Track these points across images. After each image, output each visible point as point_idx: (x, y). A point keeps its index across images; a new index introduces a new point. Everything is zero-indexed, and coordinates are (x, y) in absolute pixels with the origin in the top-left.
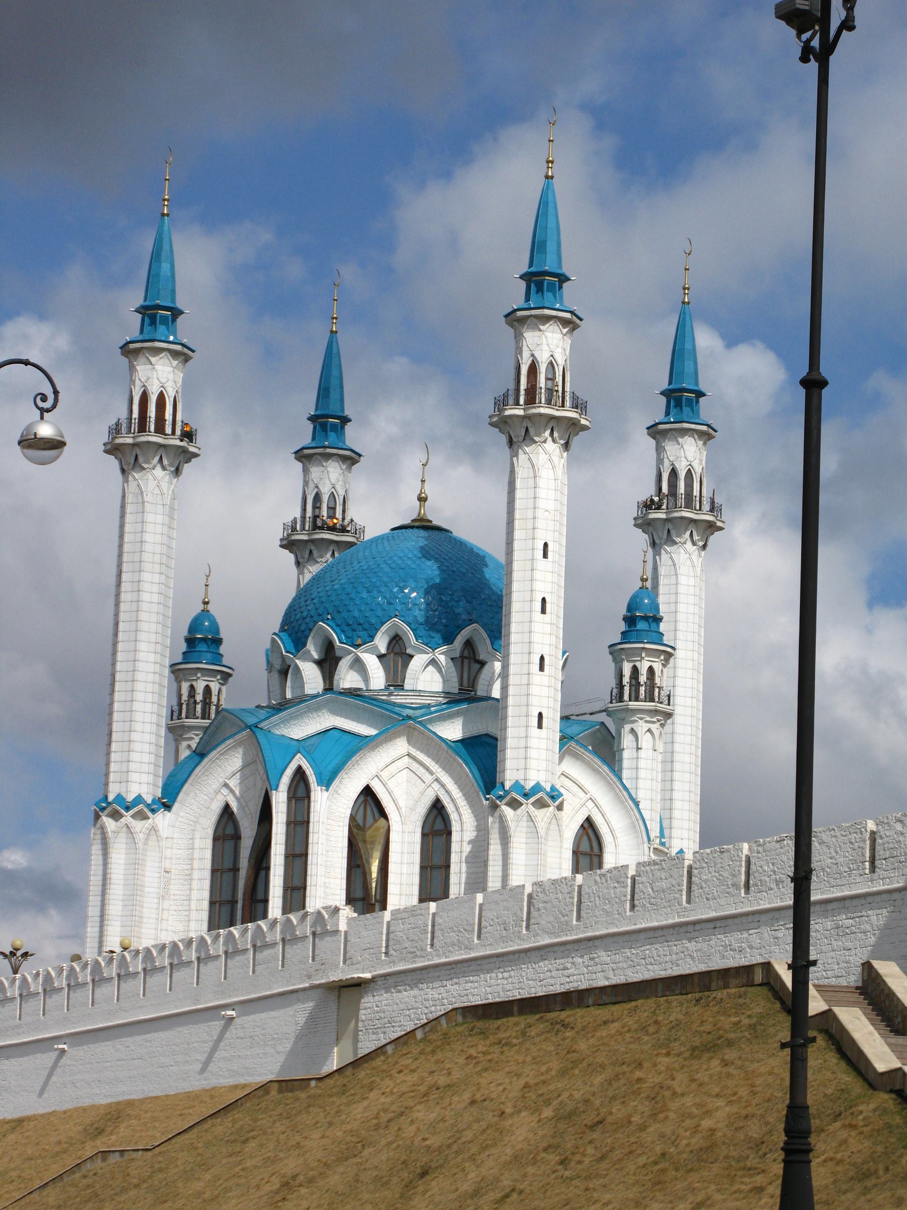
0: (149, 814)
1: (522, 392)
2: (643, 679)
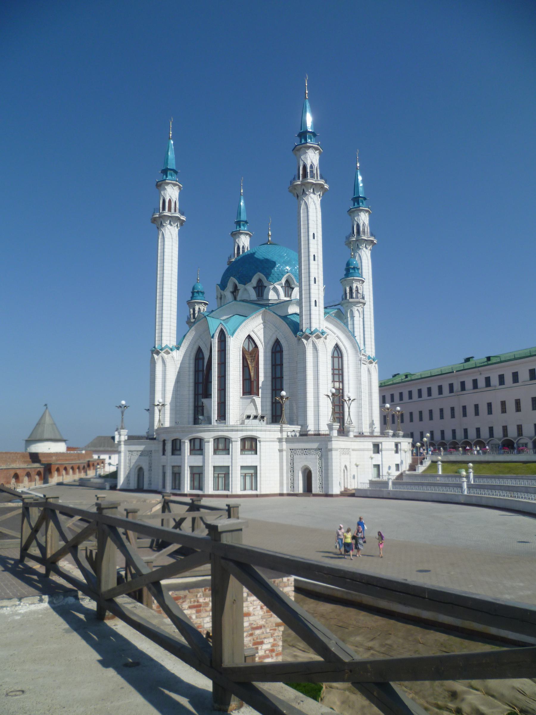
0: (170, 352)
1: (301, 175)
2: (354, 291)
